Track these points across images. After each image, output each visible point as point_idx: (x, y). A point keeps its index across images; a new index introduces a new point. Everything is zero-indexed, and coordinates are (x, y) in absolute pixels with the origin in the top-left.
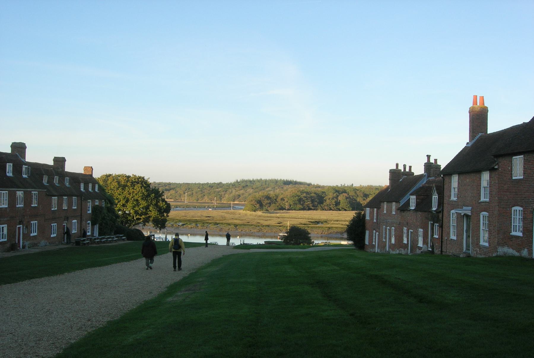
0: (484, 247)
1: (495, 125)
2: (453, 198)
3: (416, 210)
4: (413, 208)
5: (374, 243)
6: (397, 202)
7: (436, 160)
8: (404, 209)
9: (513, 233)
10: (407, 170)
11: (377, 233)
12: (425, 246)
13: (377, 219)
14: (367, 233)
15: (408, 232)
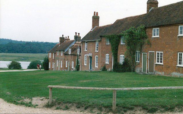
0: (97, 68)
1: (102, 23)
4: (70, 54)
5: (53, 68)
6: (64, 51)
8: (66, 54)
9: (106, 63)
10: (67, 38)
13: (54, 58)
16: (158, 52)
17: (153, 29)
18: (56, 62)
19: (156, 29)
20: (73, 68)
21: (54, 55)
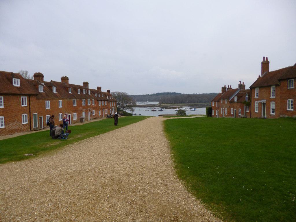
3: (237, 102)
6: (228, 99)
7: (243, 83)
8: (232, 102)
13: (218, 106)
20: (240, 115)
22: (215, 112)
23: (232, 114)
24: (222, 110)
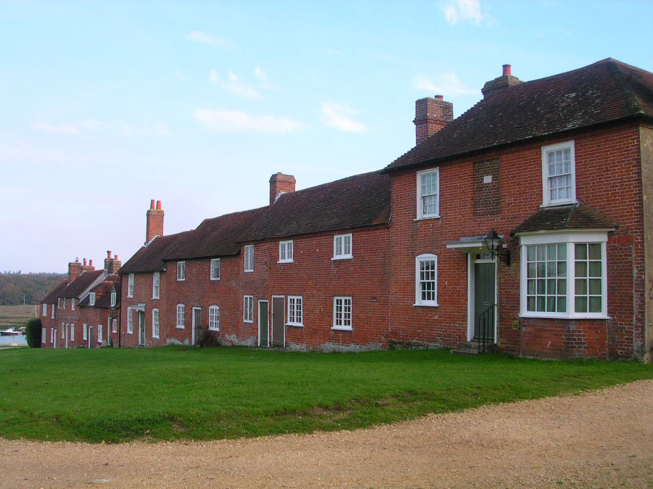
0: (156, 339)
1: (171, 228)
2: (130, 296)
3: (95, 307)
4: (93, 305)
5: (52, 342)
6: (77, 298)
7: (116, 256)
8: (84, 305)
9: (178, 326)
10: (88, 264)
11: (56, 331)
12: (105, 341)
13: (55, 316)
14: (44, 331)
15: (88, 329)
16: (292, 297)
17: (281, 243)
18: (59, 328)
19: (286, 243)
20: (101, 341)
21: (53, 308)
22: (48, 338)
23: (85, 338)
24: (88, 331)
